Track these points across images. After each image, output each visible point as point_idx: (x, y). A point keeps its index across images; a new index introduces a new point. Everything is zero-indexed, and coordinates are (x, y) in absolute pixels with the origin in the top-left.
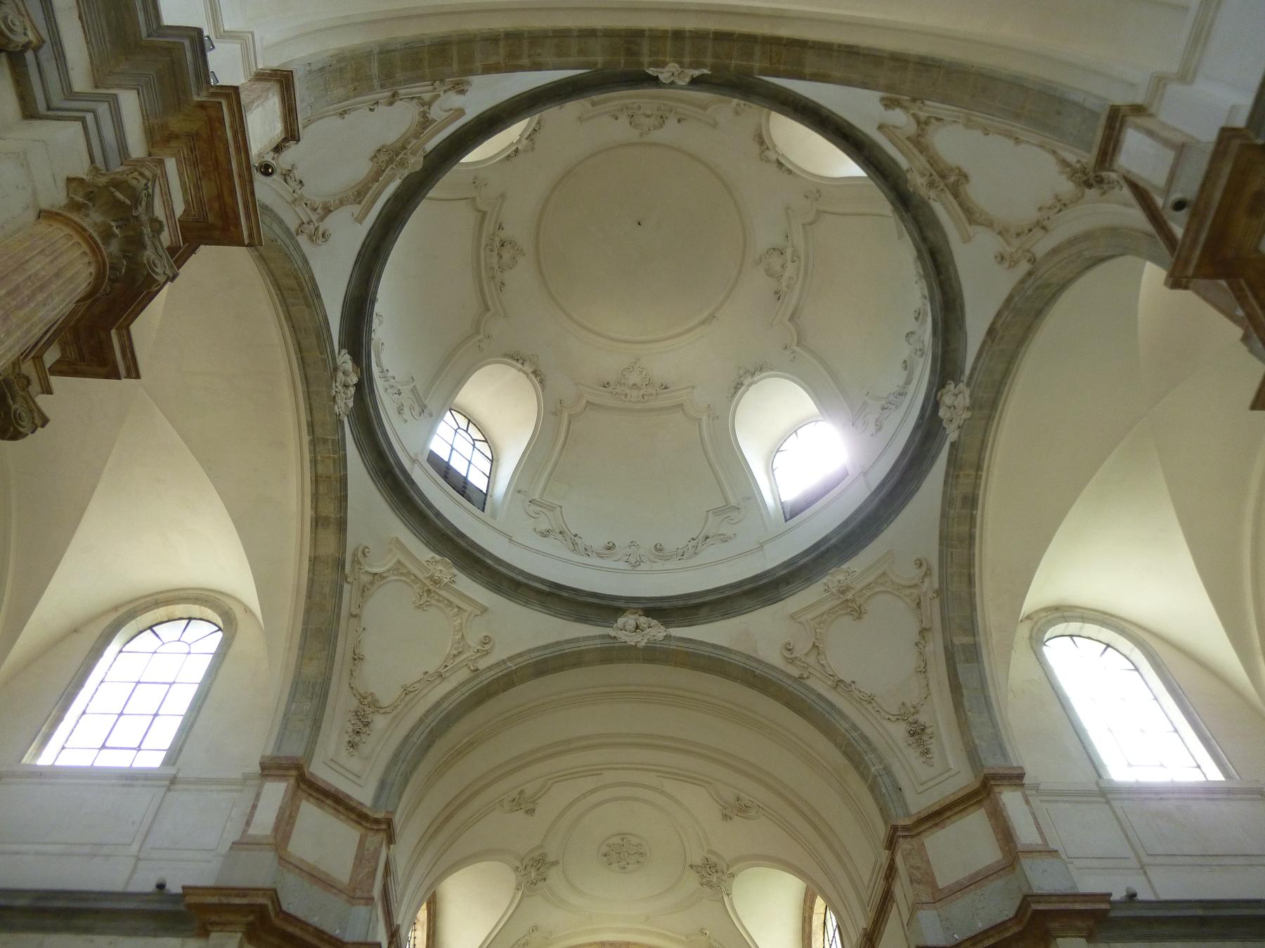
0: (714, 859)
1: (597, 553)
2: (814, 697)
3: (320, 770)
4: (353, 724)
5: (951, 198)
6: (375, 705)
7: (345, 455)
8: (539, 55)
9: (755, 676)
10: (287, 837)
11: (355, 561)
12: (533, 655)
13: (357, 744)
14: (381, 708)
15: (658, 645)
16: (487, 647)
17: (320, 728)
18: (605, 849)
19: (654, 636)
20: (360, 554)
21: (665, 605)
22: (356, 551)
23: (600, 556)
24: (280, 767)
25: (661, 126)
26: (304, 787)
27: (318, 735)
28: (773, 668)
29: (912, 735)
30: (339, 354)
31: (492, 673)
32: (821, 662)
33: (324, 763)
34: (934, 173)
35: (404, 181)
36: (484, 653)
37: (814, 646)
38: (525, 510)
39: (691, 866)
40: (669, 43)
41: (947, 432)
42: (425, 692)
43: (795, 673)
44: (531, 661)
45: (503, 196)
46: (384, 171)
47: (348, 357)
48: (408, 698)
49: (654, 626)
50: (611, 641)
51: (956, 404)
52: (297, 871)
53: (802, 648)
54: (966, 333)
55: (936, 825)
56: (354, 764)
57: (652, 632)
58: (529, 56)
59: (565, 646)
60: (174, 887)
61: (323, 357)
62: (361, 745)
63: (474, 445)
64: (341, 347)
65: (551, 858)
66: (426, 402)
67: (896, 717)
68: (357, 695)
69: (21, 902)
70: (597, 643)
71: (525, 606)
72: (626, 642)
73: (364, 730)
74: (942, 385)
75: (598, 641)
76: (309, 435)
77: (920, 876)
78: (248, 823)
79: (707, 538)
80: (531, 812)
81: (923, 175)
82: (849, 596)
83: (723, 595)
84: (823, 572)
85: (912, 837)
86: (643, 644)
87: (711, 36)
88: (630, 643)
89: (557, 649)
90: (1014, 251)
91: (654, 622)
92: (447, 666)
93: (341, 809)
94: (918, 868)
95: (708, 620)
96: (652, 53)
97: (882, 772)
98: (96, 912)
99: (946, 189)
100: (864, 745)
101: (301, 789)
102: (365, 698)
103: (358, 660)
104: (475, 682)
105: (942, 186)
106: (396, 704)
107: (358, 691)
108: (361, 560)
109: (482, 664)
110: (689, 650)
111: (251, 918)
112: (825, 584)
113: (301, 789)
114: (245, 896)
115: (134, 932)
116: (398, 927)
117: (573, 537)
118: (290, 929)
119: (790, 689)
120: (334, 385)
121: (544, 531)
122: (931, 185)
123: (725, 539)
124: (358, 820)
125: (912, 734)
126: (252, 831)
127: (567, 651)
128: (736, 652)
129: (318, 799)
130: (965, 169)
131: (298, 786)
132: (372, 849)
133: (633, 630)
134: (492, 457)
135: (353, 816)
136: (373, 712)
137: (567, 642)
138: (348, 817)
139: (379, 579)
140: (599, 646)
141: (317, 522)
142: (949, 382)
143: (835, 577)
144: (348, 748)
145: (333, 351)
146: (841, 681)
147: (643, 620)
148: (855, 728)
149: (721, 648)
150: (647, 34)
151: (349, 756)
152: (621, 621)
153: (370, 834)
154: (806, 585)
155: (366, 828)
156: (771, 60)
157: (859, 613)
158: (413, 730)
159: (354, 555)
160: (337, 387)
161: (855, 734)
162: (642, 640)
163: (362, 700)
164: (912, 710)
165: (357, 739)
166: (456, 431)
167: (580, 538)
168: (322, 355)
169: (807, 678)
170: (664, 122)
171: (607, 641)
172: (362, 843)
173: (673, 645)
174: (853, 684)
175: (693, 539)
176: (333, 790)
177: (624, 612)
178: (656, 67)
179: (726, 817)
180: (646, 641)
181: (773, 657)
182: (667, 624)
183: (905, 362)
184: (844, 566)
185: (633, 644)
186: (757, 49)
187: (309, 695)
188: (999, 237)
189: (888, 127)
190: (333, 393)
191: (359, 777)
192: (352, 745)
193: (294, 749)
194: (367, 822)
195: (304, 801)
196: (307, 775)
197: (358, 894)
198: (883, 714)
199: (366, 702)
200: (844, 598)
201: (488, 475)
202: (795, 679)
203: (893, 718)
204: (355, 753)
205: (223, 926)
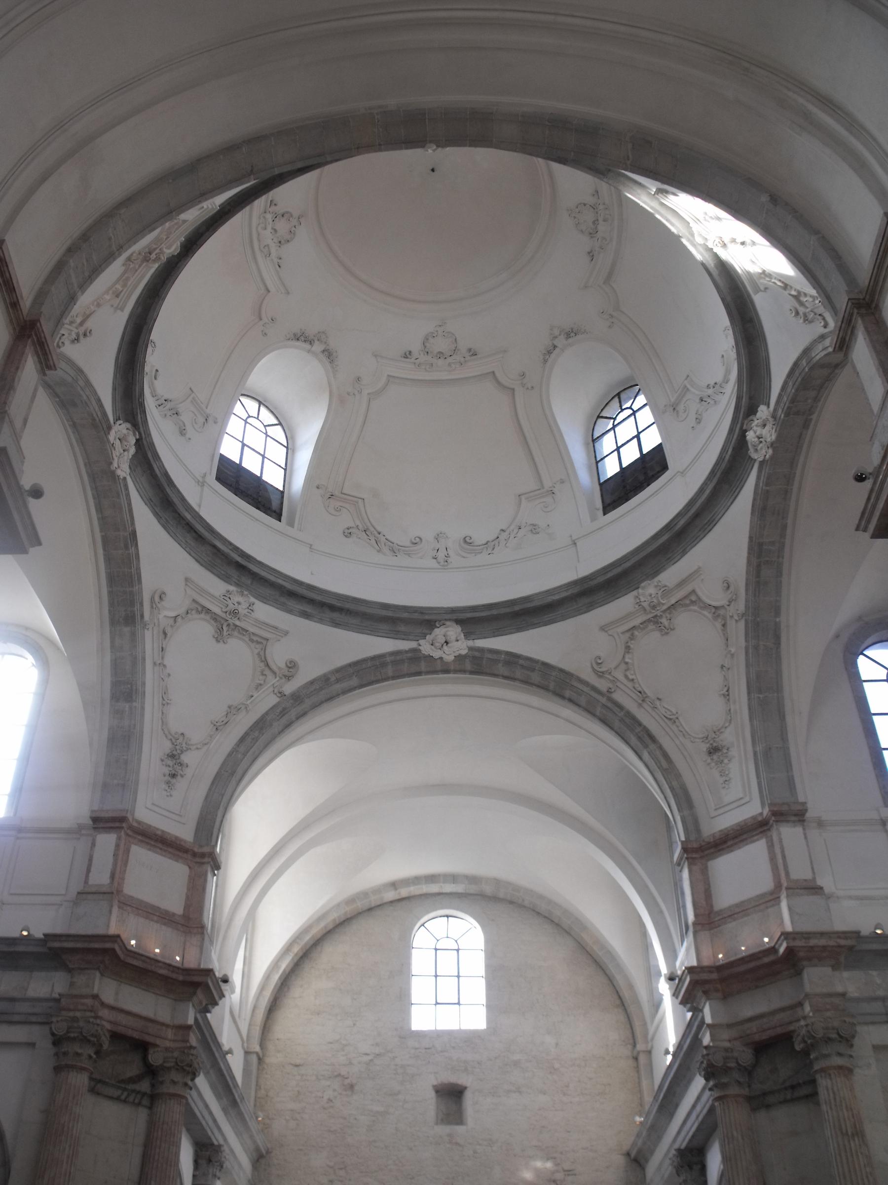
25: (426, 339)
34: (238, 623)
35: (656, 573)
45: (586, 287)
46: (669, 608)
74: (139, 443)
81: (245, 615)
90: (161, 617)
99: (223, 615)
105: (228, 617)
122: (235, 613)
130: (221, 644)
170: (425, 347)
188: (173, 614)
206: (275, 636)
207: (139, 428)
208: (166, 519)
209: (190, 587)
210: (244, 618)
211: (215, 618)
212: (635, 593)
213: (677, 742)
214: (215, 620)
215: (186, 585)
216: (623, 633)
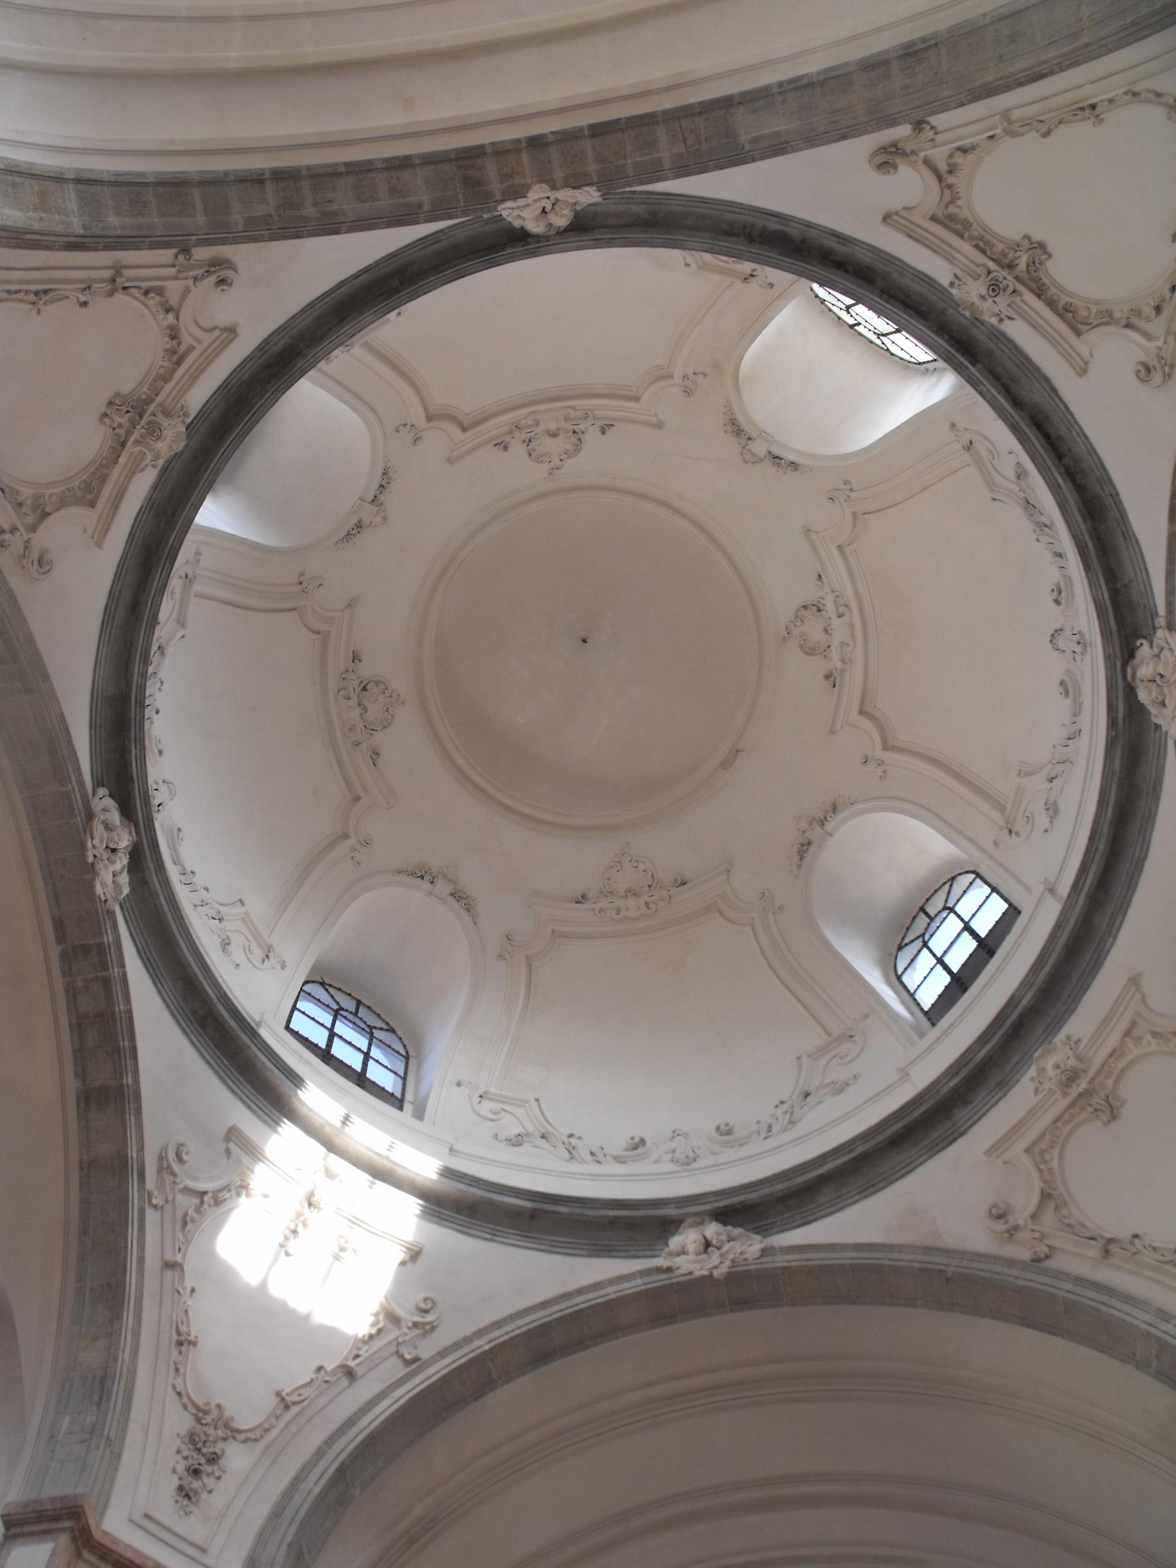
1: (614, 1157)
2: (1069, 1286)
4: (186, 1458)
5: (1029, 297)
6: (232, 1432)
7: (125, 974)
8: (330, 201)
9: (948, 1280)
11: (164, 1168)
12: (519, 1323)
13: (196, 1493)
15: (753, 1267)
16: (430, 1318)
17: (119, 1456)
19: (741, 1253)
20: (172, 1156)
21: (752, 1196)
22: (165, 1149)
23: (619, 1160)
28: (977, 1256)
31: (447, 1360)
32: (1066, 1221)
33: (131, 1521)
35: (165, 470)
36: (428, 1327)
37: (1045, 1196)
38: (473, 1108)
40: (525, 157)
41: (1164, 729)
42: (322, 1401)
43: (1024, 1254)
44: (518, 1332)
47: (110, 803)
48: (289, 1415)
50: (664, 1276)
51: (1161, 669)
53: (1024, 1203)
54: (1137, 540)
57: (737, 1246)
58: (316, 204)
62: (204, 1496)
63: (371, 1034)
64: (98, 784)
68: (190, 1407)
70: (639, 1284)
71: (491, 1240)
72: (691, 1273)
73: (209, 1469)
74: (1129, 654)
75: (639, 1281)
76: (59, 943)
81: (977, 277)
82: (1083, 1084)
83: (853, 1155)
86: (724, 1269)
87: (586, 132)
88: (697, 1273)
91: (737, 1231)
92: (357, 1356)
96: (504, 177)
102: (206, 1412)
103: (186, 1345)
106: (266, 1426)
107: (189, 1398)
108: (176, 1167)
109: (427, 1349)
110: (811, 1263)
112: (1032, 1079)
119: (1020, 1283)
120: (89, 844)
122: (995, 288)
128: (901, 1248)
131: (79, 1555)
133: (702, 1249)
134: (407, 1053)
136: (224, 1439)
137: (580, 1292)
139: (212, 1202)
140: (643, 1288)
141: (87, 1100)
142: (1138, 643)
149: (871, 1247)
150: (489, 150)
151: (182, 1513)
152: (675, 1242)
154: (1000, 1094)
156: (685, 140)
157: (1112, 1111)
158: (307, 1469)
159: (161, 1158)
162: (721, 1263)
163: (201, 1414)
165: (196, 1484)
167: (579, 1138)
168: (63, 785)
169: (1047, 1257)
173: (780, 1261)
177: (678, 1228)
178: (515, 199)
180: (728, 1263)
183: (1062, 683)
184: (1061, 1036)
185: (705, 1272)
186: (661, 132)
187: (96, 1398)
189: (897, 213)
190: (90, 859)
191: (204, 1551)
196: (97, 1535)
199: (208, 1419)
200: (1074, 1091)
201: (402, 1075)
202: (1023, 1265)
204: (196, 1511)
206: (914, 219)
207: (1125, 688)
208: (1103, 491)
209: (1082, 359)
210: (978, 270)
211: (1039, 291)
212: (189, 420)
213: (17, 275)
214: (1038, 281)
215: (1086, 363)
216: (191, 348)
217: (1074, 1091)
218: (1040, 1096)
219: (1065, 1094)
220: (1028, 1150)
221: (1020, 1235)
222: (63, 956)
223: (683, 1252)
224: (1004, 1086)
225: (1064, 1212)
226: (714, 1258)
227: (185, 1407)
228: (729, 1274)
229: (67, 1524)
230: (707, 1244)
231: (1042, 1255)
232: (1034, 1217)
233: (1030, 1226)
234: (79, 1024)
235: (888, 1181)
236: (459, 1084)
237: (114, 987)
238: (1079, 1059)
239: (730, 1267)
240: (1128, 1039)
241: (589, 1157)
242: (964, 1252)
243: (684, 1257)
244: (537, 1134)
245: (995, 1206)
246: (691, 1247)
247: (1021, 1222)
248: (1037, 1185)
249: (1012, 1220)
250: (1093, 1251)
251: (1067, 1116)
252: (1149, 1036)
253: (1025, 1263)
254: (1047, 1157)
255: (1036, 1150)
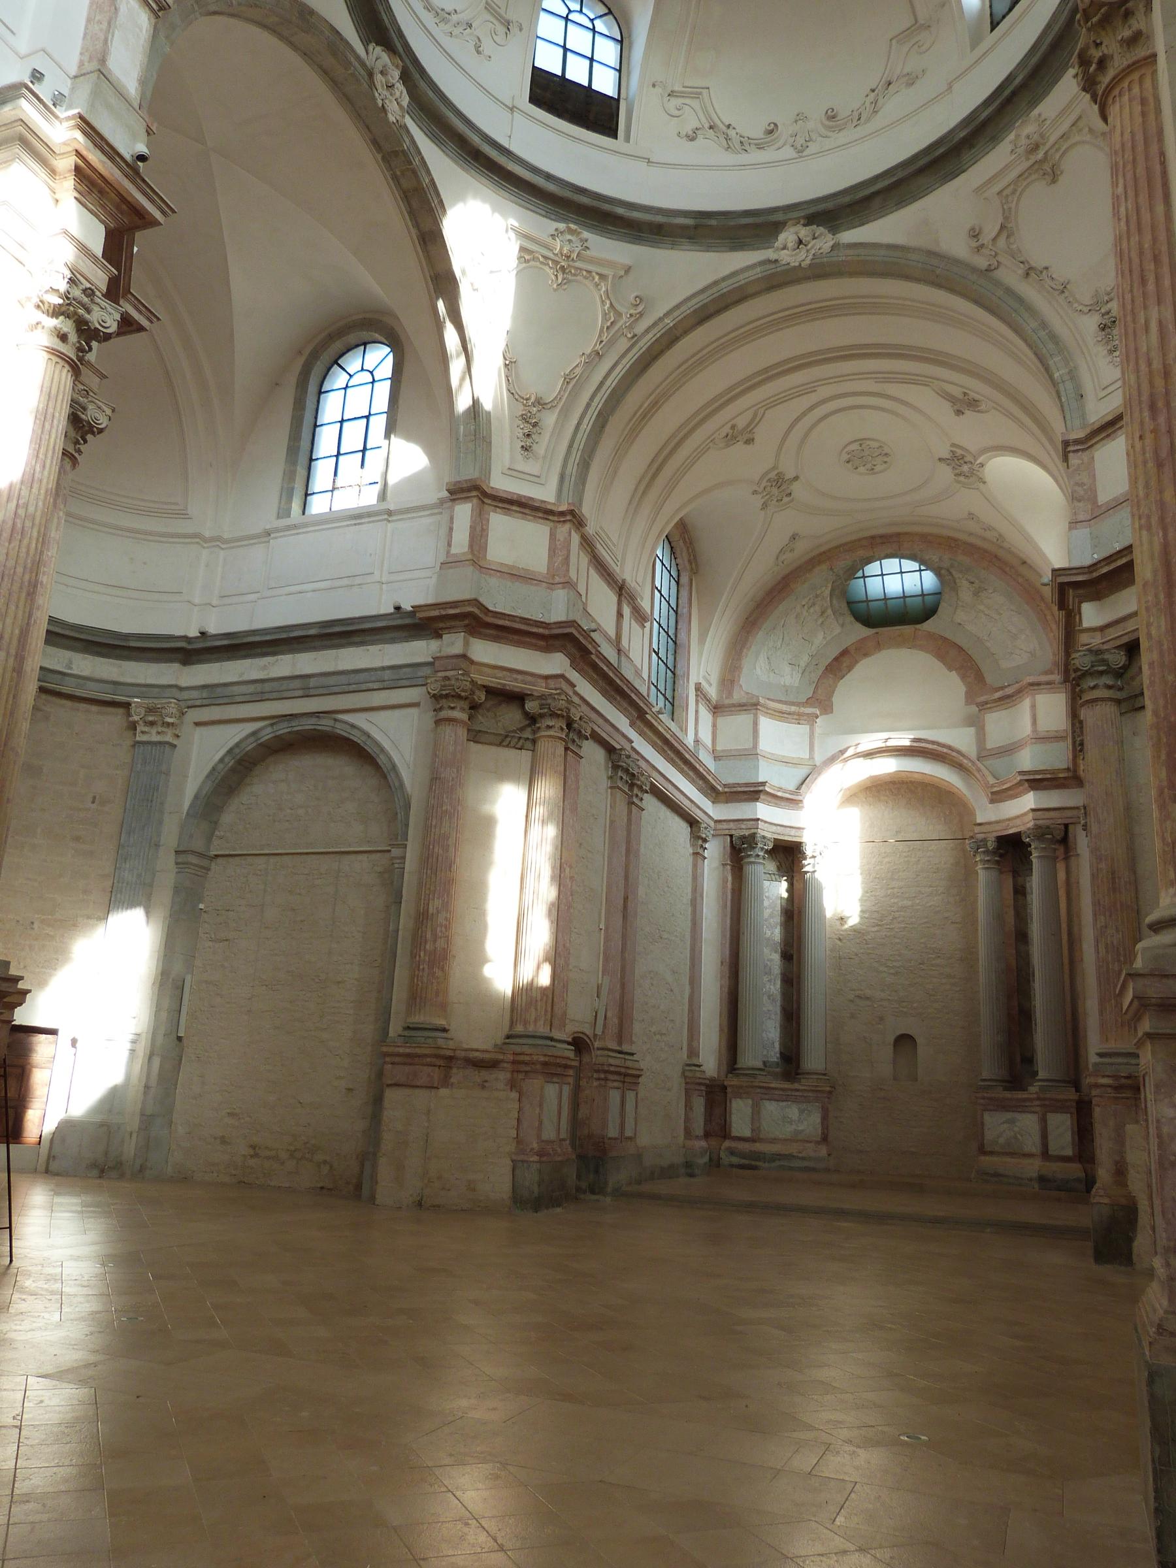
0: (959, 452)
3: (500, 483)
7: (422, 158)
10: (484, 548)
12: (690, 304)
14: (546, 404)
16: (640, 308)
18: (845, 457)
21: (830, 205)
23: (760, 147)
24: (462, 490)
26: (486, 500)
27: (490, 451)
28: (957, 262)
29: (1103, 329)
30: (367, 53)
31: (650, 335)
37: (1003, 227)
39: (940, 459)
44: (688, 312)
47: (379, 49)
48: (571, 386)
49: (821, 235)
50: (773, 266)
52: (498, 574)
55: (1108, 436)
56: (532, 467)
57: (818, 244)
59: (723, 285)
60: (407, 606)
61: (350, 72)
64: (366, 43)
65: (790, 475)
66: (508, 17)
67: (1089, 308)
69: (312, 632)
72: (788, 264)
75: (759, 269)
76: (378, 153)
77: (1082, 493)
78: (449, 545)
79: (890, 84)
80: (750, 441)
82: (1040, 155)
83: (894, 179)
84: (1009, 127)
85: (1083, 450)
86: (808, 262)
89: (715, 289)
92: (602, 342)
93: (527, 511)
94: (1082, 484)
95: (883, 212)
97: (1066, 378)
98: (363, 631)
100: (1051, 346)
101: (487, 504)
104: (634, 350)
109: (640, 328)
111: (467, 622)
113: (487, 504)
114: (456, 607)
115: (393, 641)
116: (624, 581)
117: (724, 128)
118: (501, 622)
120: (377, 95)
121: (690, 133)
123: (911, 80)
124: (545, 516)
125: (1103, 328)
126: (454, 551)
127: (725, 290)
129: (504, 508)
132: (562, 539)
135: (541, 515)
137: (724, 279)
138: (535, 516)
140: (760, 275)
143: (1024, 131)
144: (522, 452)
145: (358, 57)
146: (1031, 268)
147: (804, 232)
148: (1044, 325)
152: (782, 237)
153: (559, 525)
155: (553, 521)
157: (1053, 176)
160: (381, 93)
161: (1042, 333)
162: (807, 257)
164: (1106, 298)
166: (567, 19)
167: (734, 128)
171: (768, 267)
172: (553, 536)
174: (1045, 272)
175: (873, 91)
176: (515, 498)
179: (959, 412)
180: (811, 257)
181: (957, 246)
182: (834, 230)
184: (1036, 112)
185: (797, 264)
190: (380, 103)
191: (539, 477)
192: (525, 448)
193: (470, 473)
194: (554, 515)
195: (492, 514)
196: (489, 491)
197: (557, 580)
198: (1076, 305)
200: (1033, 159)
203: (1086, 309)
205: (450, 629)
217: (1033, 159)
218: (1014, 156)
219: (1028, 159)
220: (999, 193)
221: (983, 251)
222: (383, 158)
223: (784, 248)
224: (995, 140)
225: (1012, 240)
226: (802, 254)
227: (517, 400)
228: (810, 264)
229: (474, 493)
230: (800, 242)
231: (993, 268)
232: (994, 239)
233: (990, 247)
234: (406, 197)
235: (915, 198)
236: (654, 86)
237: (419, 174)
238: (1042, 136)
239: (813, 259)
240: (1074, 128)
241: (738, 146)
242: (949, 259)
243: (785, 251)
244: (707, 126)
245: (973, 229)
246: (790, 245)
247: (985, 242)
248: (1000, 220)
249: (981, 242)
250: (1021, 271)
251: (1027, 174)
252: (1087, 129)
253: (981, 271)
254: (1010, 198)
255: (1005, 193)
